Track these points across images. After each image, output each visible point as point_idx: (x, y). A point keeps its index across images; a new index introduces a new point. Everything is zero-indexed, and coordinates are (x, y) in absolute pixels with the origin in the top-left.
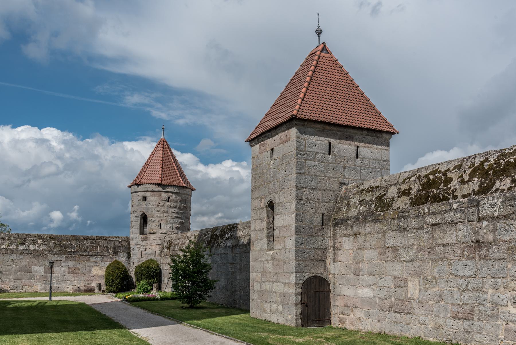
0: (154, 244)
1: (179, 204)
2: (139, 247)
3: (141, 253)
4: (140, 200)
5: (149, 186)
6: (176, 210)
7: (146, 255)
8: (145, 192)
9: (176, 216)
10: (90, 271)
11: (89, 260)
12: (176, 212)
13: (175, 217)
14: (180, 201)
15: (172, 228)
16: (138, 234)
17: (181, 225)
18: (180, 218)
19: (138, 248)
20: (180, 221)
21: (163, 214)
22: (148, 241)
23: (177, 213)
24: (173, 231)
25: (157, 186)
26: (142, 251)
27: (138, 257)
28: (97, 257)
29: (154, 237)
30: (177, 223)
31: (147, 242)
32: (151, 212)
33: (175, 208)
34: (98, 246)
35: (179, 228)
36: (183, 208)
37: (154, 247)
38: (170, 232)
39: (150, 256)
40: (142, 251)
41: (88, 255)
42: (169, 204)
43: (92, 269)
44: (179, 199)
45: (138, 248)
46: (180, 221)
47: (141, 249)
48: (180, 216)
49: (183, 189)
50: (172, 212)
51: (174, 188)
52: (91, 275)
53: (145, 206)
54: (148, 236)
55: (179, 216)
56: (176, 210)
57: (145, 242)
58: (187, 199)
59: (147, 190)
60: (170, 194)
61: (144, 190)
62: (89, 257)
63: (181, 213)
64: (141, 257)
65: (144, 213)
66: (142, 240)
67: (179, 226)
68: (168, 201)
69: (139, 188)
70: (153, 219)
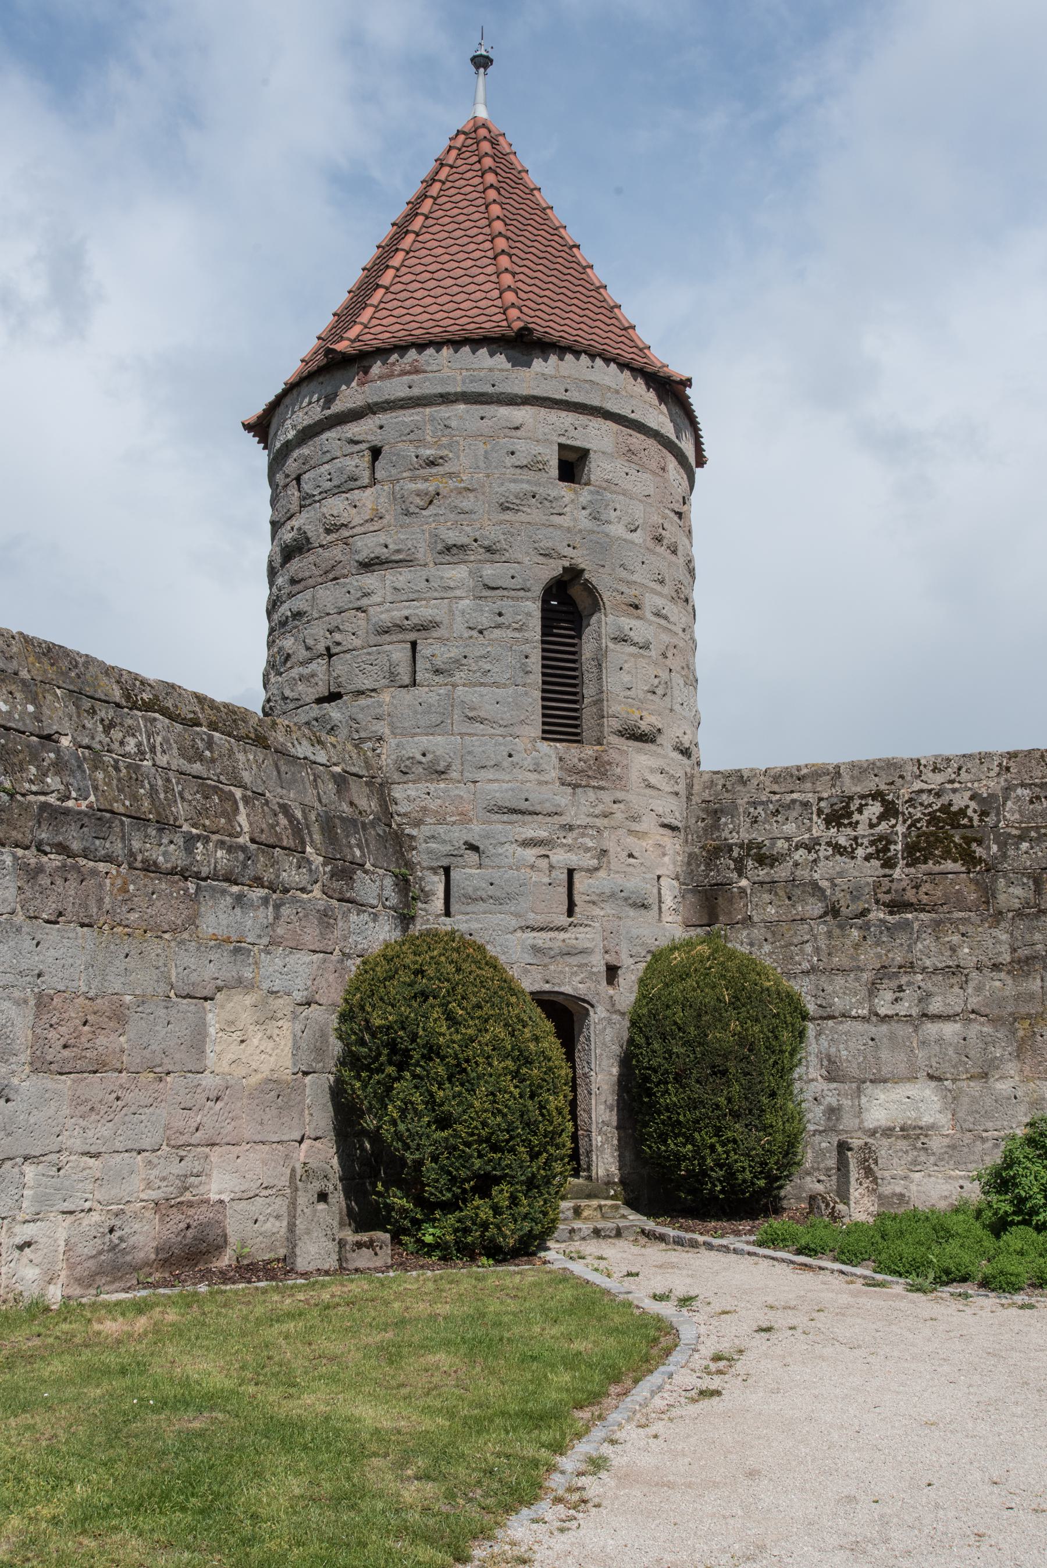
0: (650, 823)
2: (543, 834)
3: (564, 890)
4: (535, 466)
5: (610, 375)
7: (609, 909)
8: (583, 419)
10: (198, 1041)
11: (192, 920)
16: (535, 729)
19: (527, 843)
22: (620, 795)
25: (651, 396)
26: (571, 872)
27: (532, 919)
28: (239, 898)
29: (652, 771)
31: (607, 797)
32: (624, 574)
34: (238, 793)
37: (648, 843)
39: (632, 912)
40: (571, 872)
41: (184, 874)
43: (213, 1018)
45: (527, 843)
47: (560, 857)
52: (207, 1080)
53: (583, 520)
54: (614, 755)
57: (591, 794)
59: (596, 403)
61: (575, 396)
62: (192, 887)
64: (563, 920)
65: (573, 575)
66: (573, 779)
69: (523, 372)
70: (639, 629)
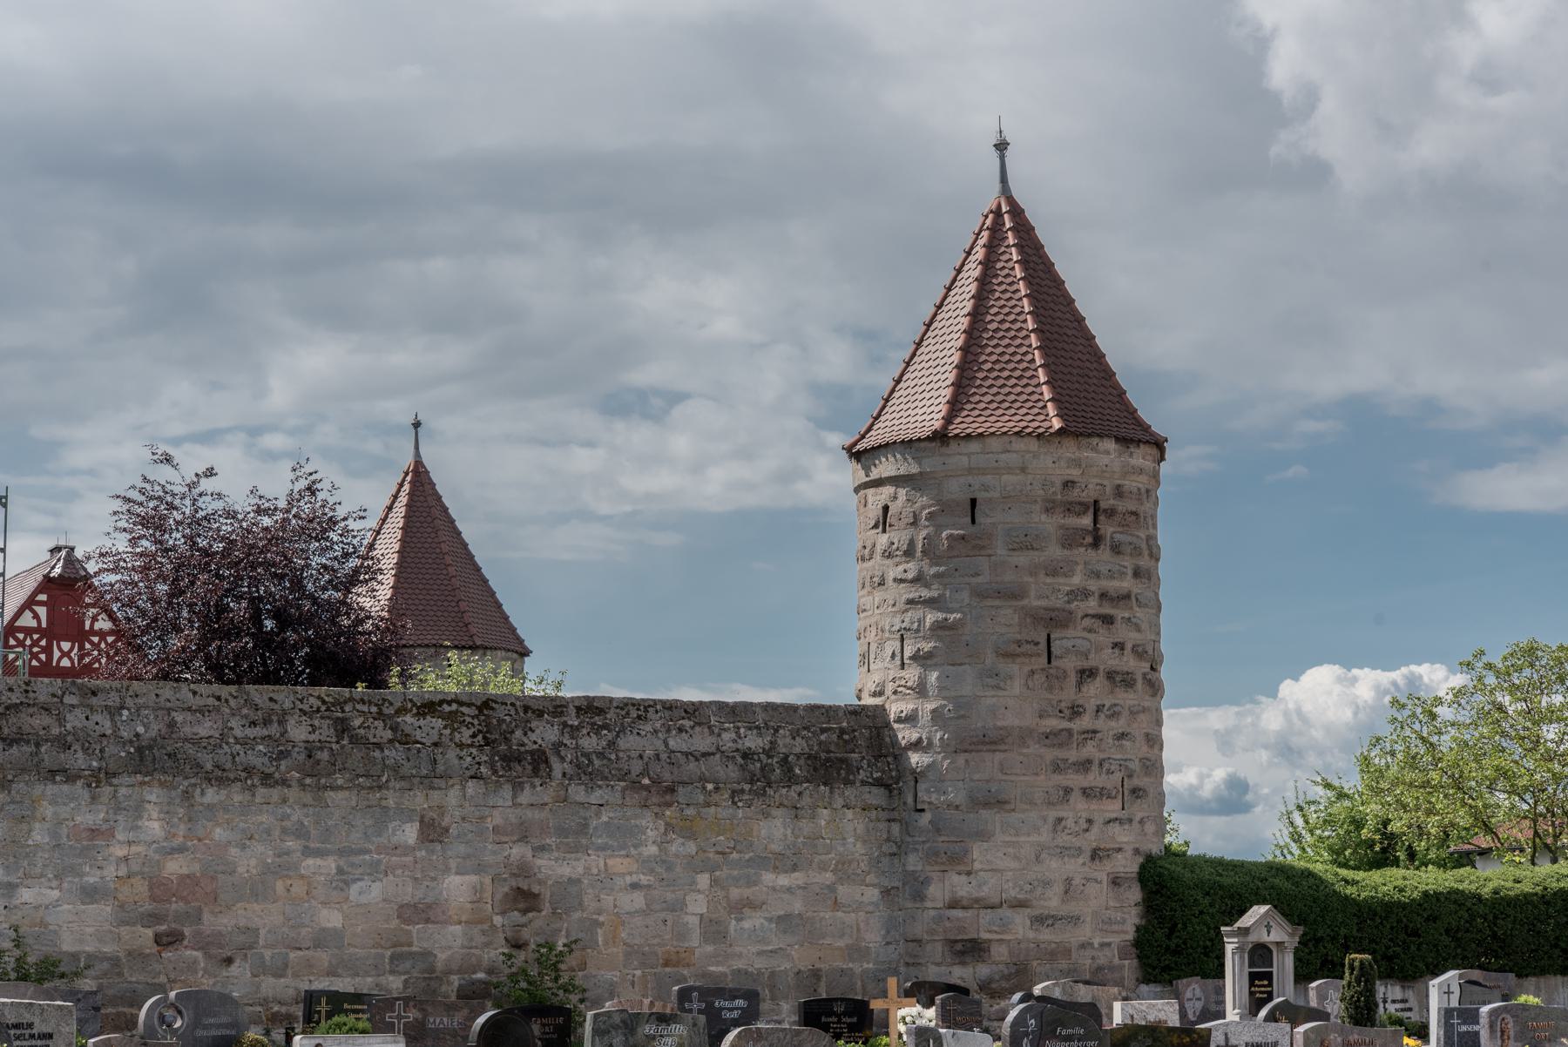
1: (924, 533)
6: (912, 569)
9: (911, 596)
12: (910, 576)
13: (910, 602)
14: (931, 516)
15: (898, 658)
17: (939, 638)
18: (931, 603)
20: (931, 617)
21: (871, 598)
23: (914, 581)
24: (903, 673)
30: (918, 631)
33: (909, 553)
35: (930, 655)
36: (950, 547)
38: (894, 680)
42: (883, 540)
44: (923, 508)
46: (931, 617)
48: (935, 594)
49: (944, 450)
50: (895, 580)
51: (898, 456)
55: (925, 593)
56: (912, 569)
58: (980, 496)
60: (888, 490)
63: (937, 576)
67: (927, 646)
68: (884, 531)
